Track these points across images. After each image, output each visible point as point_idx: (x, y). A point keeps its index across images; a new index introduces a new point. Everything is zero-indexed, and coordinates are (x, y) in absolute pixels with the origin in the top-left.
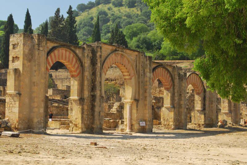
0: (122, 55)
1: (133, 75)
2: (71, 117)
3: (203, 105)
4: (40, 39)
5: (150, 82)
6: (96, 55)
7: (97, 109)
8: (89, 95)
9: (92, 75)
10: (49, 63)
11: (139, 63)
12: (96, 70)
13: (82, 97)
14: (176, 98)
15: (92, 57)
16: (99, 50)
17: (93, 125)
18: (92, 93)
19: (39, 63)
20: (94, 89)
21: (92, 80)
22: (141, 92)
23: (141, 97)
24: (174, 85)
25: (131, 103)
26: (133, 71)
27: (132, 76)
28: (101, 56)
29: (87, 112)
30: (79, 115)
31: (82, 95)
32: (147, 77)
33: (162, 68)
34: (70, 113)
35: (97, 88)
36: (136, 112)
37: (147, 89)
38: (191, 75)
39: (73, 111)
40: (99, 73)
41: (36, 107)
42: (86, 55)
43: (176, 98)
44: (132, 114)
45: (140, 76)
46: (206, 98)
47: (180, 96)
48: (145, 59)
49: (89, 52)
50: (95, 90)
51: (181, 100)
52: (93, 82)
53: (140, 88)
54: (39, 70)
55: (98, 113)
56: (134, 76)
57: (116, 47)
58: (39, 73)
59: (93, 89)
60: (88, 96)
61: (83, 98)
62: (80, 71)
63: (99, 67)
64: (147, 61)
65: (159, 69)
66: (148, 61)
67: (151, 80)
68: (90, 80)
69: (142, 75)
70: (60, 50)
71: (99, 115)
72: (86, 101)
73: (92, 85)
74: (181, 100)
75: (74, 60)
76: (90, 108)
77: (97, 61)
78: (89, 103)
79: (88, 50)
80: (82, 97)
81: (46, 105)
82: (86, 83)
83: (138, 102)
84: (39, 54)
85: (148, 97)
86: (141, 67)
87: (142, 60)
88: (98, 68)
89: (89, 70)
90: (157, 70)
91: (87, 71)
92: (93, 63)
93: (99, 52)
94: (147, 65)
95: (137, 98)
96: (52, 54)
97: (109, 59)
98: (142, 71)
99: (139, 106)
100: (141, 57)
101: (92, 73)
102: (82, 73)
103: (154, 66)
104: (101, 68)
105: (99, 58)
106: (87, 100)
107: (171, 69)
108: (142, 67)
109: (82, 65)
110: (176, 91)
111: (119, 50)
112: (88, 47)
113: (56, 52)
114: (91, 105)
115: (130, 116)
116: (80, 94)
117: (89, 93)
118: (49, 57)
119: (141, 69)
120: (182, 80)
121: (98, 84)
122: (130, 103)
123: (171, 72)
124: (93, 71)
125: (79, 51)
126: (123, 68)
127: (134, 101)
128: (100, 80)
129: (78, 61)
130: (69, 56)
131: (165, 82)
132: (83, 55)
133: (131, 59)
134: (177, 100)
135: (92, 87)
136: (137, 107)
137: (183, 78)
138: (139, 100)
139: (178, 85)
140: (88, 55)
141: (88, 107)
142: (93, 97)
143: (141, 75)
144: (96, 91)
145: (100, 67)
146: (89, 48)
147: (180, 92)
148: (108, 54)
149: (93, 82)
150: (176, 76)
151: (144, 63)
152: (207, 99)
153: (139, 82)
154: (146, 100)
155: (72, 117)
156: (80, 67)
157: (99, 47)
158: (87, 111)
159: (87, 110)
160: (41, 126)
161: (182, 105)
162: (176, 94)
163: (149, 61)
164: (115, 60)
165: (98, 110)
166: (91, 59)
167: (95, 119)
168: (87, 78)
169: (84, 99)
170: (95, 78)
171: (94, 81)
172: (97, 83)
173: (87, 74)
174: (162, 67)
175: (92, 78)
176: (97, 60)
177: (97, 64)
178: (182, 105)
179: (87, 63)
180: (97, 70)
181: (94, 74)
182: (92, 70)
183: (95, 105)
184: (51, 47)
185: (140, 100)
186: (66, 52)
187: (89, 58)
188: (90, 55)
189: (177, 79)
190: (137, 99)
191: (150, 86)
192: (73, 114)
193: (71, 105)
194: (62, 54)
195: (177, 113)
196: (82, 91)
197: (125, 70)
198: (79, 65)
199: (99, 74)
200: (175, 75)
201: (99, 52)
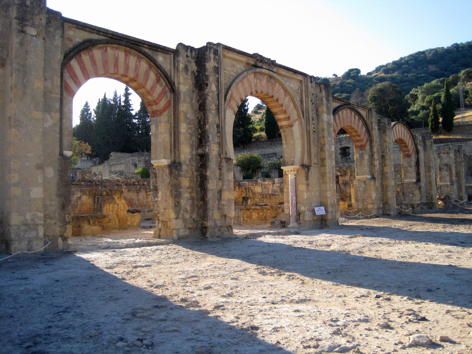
0: (271, 77)
1: (297, 118)
2: (156, 205)
3: (416, 174)
4: (27, 6)
5: (329, 132)
6: (205, 65)
7: (212, 185)
8: (192, 155)
9: (198, 111)
11: (307, 96)
12: (205, 99)
13: (175, 161)
14: (377, 163)
15: (197, 71)
16: (212, 56)
17: (204, 222)
18: (200, 151)
20: (203, 142)
21: (199, 122)
22: (314, 150)
23: (314, 160)
24: (371, 141)
25: (296, 173)
26: (295, 111)
27: (295, 121)
29: (190, 193)
30: (170, 201)
31: (175, 154)
32: (323, 121)
33: (349, 111)
34: (154, 197)
35: (210, 138)
36: (305, 189)
37: (324, 145)
38: (397, 126)
39: (158, 193)
40: (214, 105)
41: (16, 185)
42: (181, 66)
43: (377, 163)
44: (298, 193)
45: (309, 121)
46: (420, 163)
47: (382, 158)
48: (319, 89)
49: (189, 61)
50: (205, 142)
51: (385, 165)
52: (201, 124)
53: (312, 143)
54: (25, 87)
55: (216, 194)
56: (297, 120)
57: (254, 60)
58: (24, 93)
59: (202, 139)
60: (189, 157)
61: (177, 161)
62: (169, 101)
63: (213, 92)
64: (321, 91)
65: (345, 111)
66: (323, 92)
67: (331, 127)
68: (196, 122)
69: (313, 119)
70: (109, 49)
71: (220, 199)
72: (184, 167)
73: (200, 132)
74: (385, 165)
75: (152, 76)
76: (198, 183)
77: (207, 80)
78: (195, 173)
79: (187, 56)
80: (175, 161)
81: (61, 179)
82: (183, 128)
83: (308, 170)
84: (21, 44)
85: (327, 160)
86: (310, 103)
87: (311, 90)
88: (210, 94)
89: (192, 100)
90: (340, 112)
91: (184, 101)
93: (212, 60)
94: (322, 100)
95: (306, 162)
96: (85, 57)
97: (242, 81)
98: (312, 110)
99: (310, 178)
100: (310, 84)
101: (198, 106)
102: (174, 107)
103: (336, 105)
104: (218, 95)
105: (213, 74)
106: (188, 165)
107: (365, 113)
108: (313, 104)
109: (172, 88)
110: (375, 150)
111: (264, 67)
114: (199, 177)
115: (294, 198)
116: (171, 152)
117: (192, 150)
118: (74, 63)
119: (311, 107)
120: (385, 132)
121: (212, 130)
122: (293, 172)
123: (366, 118)
124: (200, 102)
125: (165, 58)
126: (274, 104)
127: (301, 167)
128: (217, 121)
129: (161, 79)
130: (137, 68)
131: (356, 135)
132: (176, 68)
133: (291, 88)
134: (378, 166)
135: (199, 137)
136: (307, 179)
137: (385, 128)
138: (311, 166)
139: (378, 140)
140: (186, 68)
141: (191, 181)
142: (202, 160)
143: (311, 119)
144: (208, 144)
145: (216, 93)
146: (189, 53)
147: (383, 152)
148: (240, 71)
149: (201, 124)
150: (374, 124)
151: (316, 97)
152: (422, 164)
153: (309, 132)
154: (324, 166)
155: (158, 206)
156: (168, 93)
157: (212, 50)
158: (189, 191)
159: (189, 188)
160: (38, 233)
161: (387, 173)
162: (376, 156)
163: (325, 92)
164: (256, 85)
165: (215, 187)
166: (196, 77)
167: (208, 207)
168: (186, 117)
169: (180, 163)
170: (204, 116)
171: (202, 123)
172: (211, 129)
173: (186, 107)
174: (349, 108)
175: (198, 117)
176: (207, 77)
177: (207, 85)
178: (387, 173)
180: (209, 98)
181: (202, 107)
182: (199, 100)
183: (206, 176)
184: (78, 40)
185: (313, 165)
186: (126, 55)
187: (190, 73)
188: (193, 67)
189: (375, 129)
190: (307, 164)
191: (330, 139)
192: (159, 199)
193: (154, 179)
195: (380, 189)
196: (175, 147)
197: (278, 109)
198: (167, 89)
199: (214, 107)
200: (372, 123)
201: (212, 60)
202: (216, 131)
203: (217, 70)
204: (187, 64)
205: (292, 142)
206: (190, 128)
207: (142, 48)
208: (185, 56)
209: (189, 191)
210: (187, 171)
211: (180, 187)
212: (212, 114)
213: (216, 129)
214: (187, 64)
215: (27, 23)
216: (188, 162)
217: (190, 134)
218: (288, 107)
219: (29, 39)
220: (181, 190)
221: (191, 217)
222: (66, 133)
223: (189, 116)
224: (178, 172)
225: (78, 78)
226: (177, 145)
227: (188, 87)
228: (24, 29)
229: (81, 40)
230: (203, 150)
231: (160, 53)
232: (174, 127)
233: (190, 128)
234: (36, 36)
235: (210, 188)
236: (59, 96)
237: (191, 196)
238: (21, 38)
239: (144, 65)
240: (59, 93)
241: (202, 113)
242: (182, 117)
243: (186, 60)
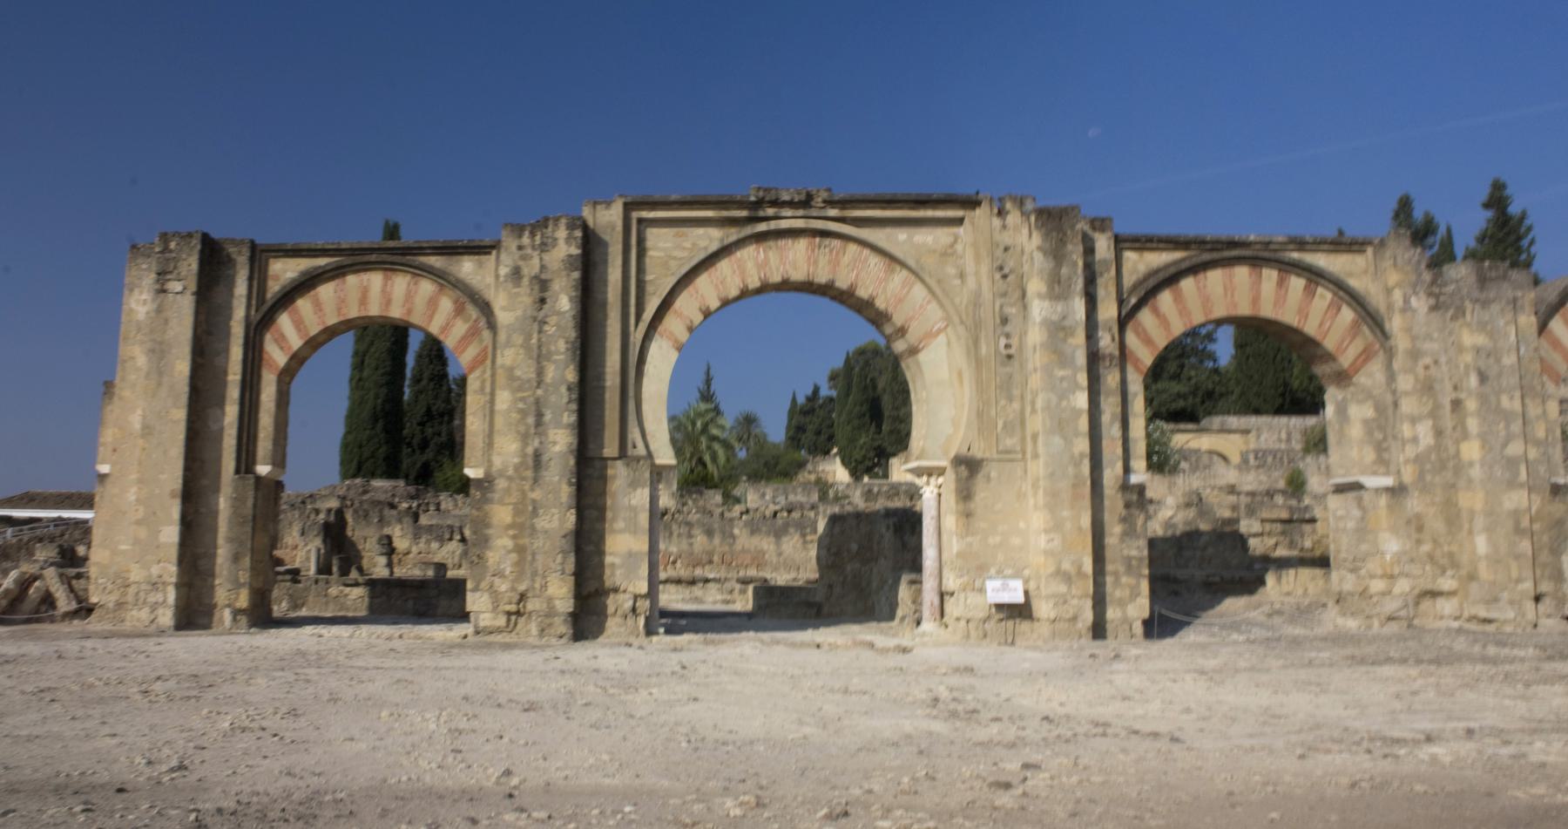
8: (524, 455)
27: (931, 335)
29: (514, 537)
63: (559, 313)
75: (446, 304)
79: (520, 248)
106: (510, 478)
113: (326, 291)
146: (526, 240)
158: (511, 532)
168: (511, 377)
187: (526, 281)
204: (521, 263)
206: (522, 399)
209: (511, 532)
210: (508, 491)
211: (488, 526)
212: (555, 362)
214: (521, 263)
216: (510, 472)
217: (521, 411)
220: (490, 531)
221: (513, 589)
223: (518, 373)
224: (483, 495)
231: (466, 257)
233: (522, 399)
237: (516, 545)
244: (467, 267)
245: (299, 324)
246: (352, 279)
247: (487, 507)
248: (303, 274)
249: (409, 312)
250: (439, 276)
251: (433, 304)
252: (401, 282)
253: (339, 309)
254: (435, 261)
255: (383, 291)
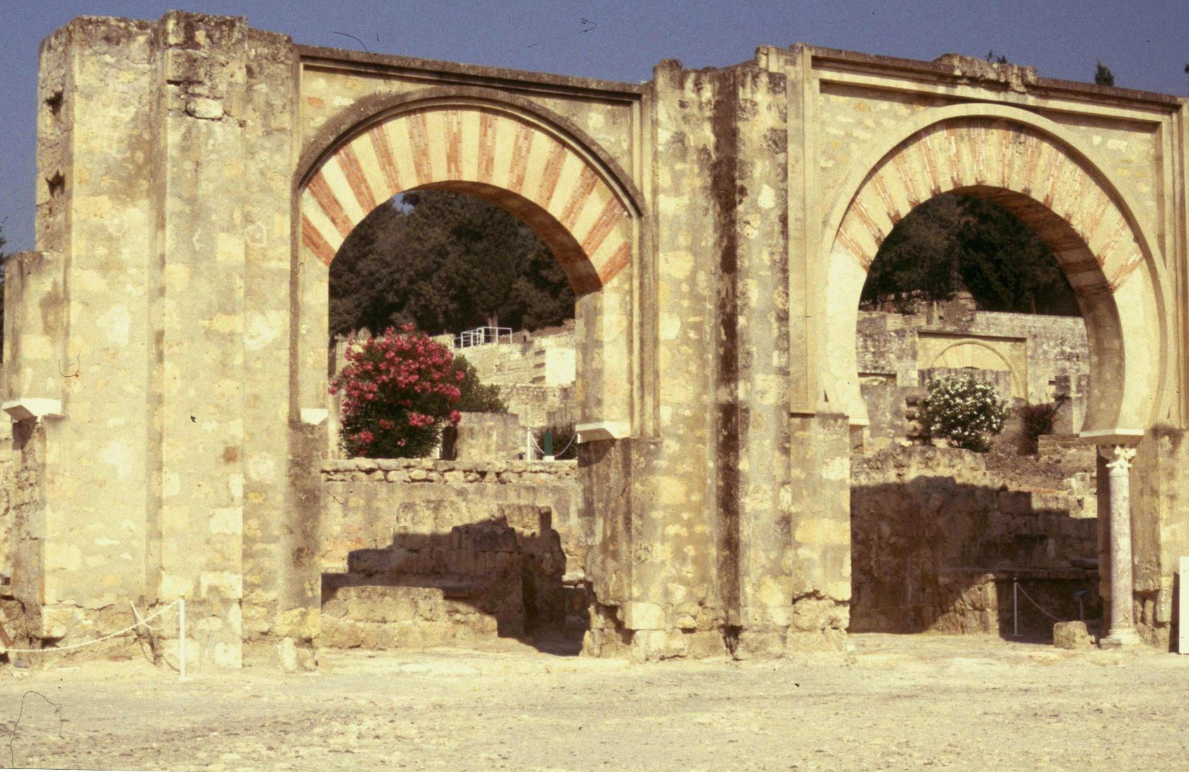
4: (197, 46)
7: (756, 502)
10: (330, 206)
18: (724, 396)
19: (192, 201)
27: (1127, 269)
28: (779, 141)
61: (650, 430)
62: (627, 247)
79: (683, 105)
81: (293, 484)
82: (669, 328)
92: (726, 186)
96: (362, 145)
106: (680, 439)
112: (681, 86)
113: (397, 130)
118: (332, 170)
130: (519, 156)
135: (721, 351)
140: (680, 138)
142: (731, 424)
145: (774, 216)
146: (689, 93)
165: (768, 505)
175: (719, 292)
177: (743, 191)
179: (677, 197)
188: (706, 135)
194: (455, 143)
202: (775, 333)
203: (779, 141)
204: (686, 128)
205: (1116, 342)
207: (533, 99)
208: (676, 104)
210: (675, 459)
213: (775, 325)
214: (686, 128)
215: (198, 90)
218: (1097, 223)
219: (204, 129)
222: (310, 361)
225: (341, 209)
226: (649, 378)
227: (685, 200)
228: (192, 106)
229: (348, 102)
230: (731, 393)
231: (595, 105)
232: (642, 324)
234: (220, 119)
235: (748, 509)
236: (287, 265)
238: (183, 130)
239: (542, 144)
240: (288, 256)
241: (726, 277)
242: (664, 295)
243: (679, 117)
244: (594, 120)
245: (357, 181)
246: (435, 119)
247: (653, 480)
248: (362, 102)
249: (520, 181)
250: (568, 136)
251: (552, 171)
252: (506, 130)
253: (418, 166)
254: (555, 106)
255: (482, 145)
